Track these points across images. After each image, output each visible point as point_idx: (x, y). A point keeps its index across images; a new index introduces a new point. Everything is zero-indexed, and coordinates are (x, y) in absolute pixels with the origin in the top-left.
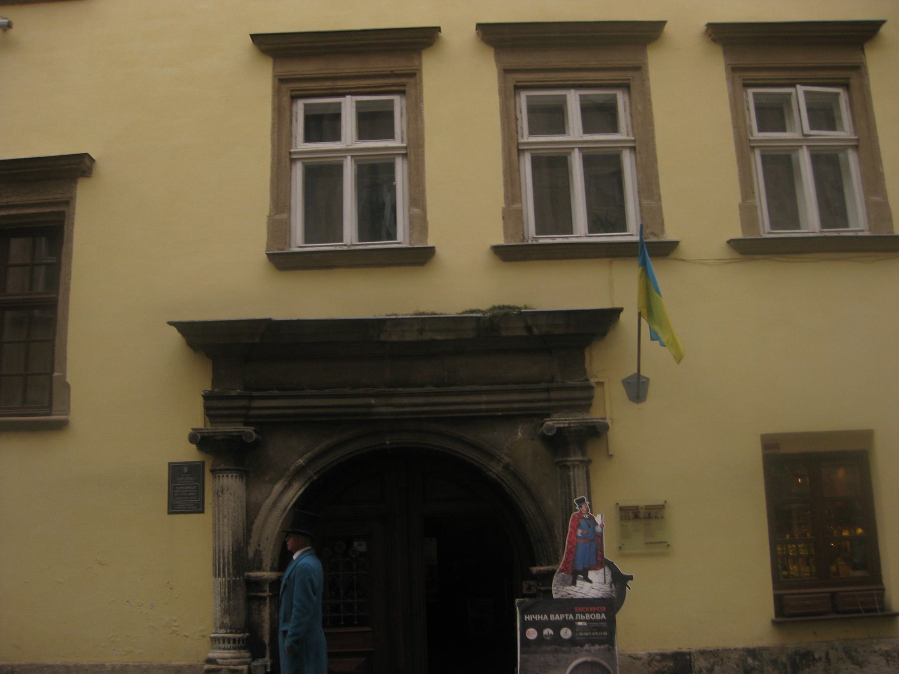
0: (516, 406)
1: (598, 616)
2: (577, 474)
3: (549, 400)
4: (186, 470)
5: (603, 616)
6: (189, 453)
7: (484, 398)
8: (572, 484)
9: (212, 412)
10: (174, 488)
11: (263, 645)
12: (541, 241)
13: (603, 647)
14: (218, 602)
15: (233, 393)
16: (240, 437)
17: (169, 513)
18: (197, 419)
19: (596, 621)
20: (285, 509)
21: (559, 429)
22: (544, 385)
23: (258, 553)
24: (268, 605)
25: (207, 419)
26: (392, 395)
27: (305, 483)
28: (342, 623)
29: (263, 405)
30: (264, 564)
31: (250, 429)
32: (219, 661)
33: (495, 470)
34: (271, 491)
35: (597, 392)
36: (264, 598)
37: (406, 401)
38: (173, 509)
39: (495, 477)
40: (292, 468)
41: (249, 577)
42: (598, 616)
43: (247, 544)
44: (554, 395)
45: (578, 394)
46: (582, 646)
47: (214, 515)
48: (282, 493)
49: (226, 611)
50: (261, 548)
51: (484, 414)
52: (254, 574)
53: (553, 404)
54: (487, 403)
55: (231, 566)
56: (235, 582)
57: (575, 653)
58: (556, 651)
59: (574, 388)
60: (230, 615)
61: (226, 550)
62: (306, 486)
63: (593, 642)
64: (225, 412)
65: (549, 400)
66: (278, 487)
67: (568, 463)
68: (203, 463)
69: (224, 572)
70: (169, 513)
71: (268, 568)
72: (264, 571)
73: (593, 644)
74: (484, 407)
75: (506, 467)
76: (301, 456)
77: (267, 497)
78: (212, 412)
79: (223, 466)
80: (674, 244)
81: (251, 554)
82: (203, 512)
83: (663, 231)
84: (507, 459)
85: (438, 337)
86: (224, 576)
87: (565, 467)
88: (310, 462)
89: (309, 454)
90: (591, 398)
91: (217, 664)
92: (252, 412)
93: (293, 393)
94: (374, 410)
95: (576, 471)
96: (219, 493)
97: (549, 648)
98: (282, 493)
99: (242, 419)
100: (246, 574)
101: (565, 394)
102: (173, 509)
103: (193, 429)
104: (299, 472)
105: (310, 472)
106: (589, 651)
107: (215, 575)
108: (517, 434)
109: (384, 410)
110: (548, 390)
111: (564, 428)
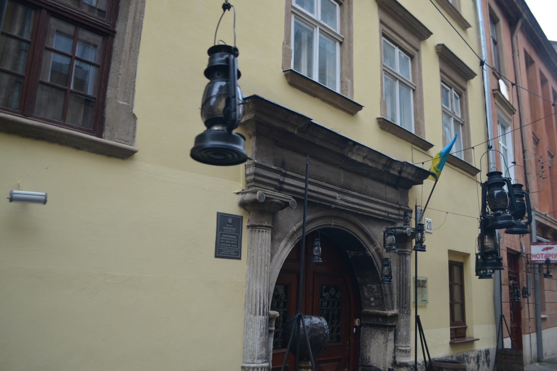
6: (232, 208)
7: (378, 207)
9: (258, 178)
17: (216, 257)
28: (280, 346)
39: (371, 255)
54: (379, 210)
67: (407, 253)
68: (242, 217)
70: (216, 257)
78: (258, 178)
82: (240, 259)
85: (370, 164)
86: (263, 315)
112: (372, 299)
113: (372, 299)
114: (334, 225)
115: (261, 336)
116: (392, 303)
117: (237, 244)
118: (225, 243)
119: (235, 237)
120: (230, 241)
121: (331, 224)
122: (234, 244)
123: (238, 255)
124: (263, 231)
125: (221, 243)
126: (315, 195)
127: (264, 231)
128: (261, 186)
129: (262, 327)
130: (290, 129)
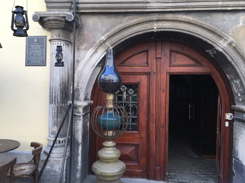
4: (36, 41)
9: (50, 5)
11: (78, 143)
14: (51, 119)
16: (65, 17)
17: (26, 66)
24: (81, 121)
30: (80, 97)
33: (221, 45)
36: (80, 116)
39: (221, 50)
40: (98, 41)
50: (79, 87)
64: (57, 5)
69: (55, 101)
70: (26, 66)
71: (83, 99)
75: (230, 44)
84: (231, 39)
86: (55, 104)
88: (109, 37)
89: (108, 34)
105: (108, 44)
108: (239, 23)
109: (155, 5)
112: (239, 95)
113: (239, 95)
114: (157, 29)
115: (53, 118)
117: (42, 56)
118: (33, 56)
121: (153, 29)
122: (39, 56)
124: (53, 44)
125: (29, 56)
126: (118, 5)
127: (54, 43)
129: (54, 112)
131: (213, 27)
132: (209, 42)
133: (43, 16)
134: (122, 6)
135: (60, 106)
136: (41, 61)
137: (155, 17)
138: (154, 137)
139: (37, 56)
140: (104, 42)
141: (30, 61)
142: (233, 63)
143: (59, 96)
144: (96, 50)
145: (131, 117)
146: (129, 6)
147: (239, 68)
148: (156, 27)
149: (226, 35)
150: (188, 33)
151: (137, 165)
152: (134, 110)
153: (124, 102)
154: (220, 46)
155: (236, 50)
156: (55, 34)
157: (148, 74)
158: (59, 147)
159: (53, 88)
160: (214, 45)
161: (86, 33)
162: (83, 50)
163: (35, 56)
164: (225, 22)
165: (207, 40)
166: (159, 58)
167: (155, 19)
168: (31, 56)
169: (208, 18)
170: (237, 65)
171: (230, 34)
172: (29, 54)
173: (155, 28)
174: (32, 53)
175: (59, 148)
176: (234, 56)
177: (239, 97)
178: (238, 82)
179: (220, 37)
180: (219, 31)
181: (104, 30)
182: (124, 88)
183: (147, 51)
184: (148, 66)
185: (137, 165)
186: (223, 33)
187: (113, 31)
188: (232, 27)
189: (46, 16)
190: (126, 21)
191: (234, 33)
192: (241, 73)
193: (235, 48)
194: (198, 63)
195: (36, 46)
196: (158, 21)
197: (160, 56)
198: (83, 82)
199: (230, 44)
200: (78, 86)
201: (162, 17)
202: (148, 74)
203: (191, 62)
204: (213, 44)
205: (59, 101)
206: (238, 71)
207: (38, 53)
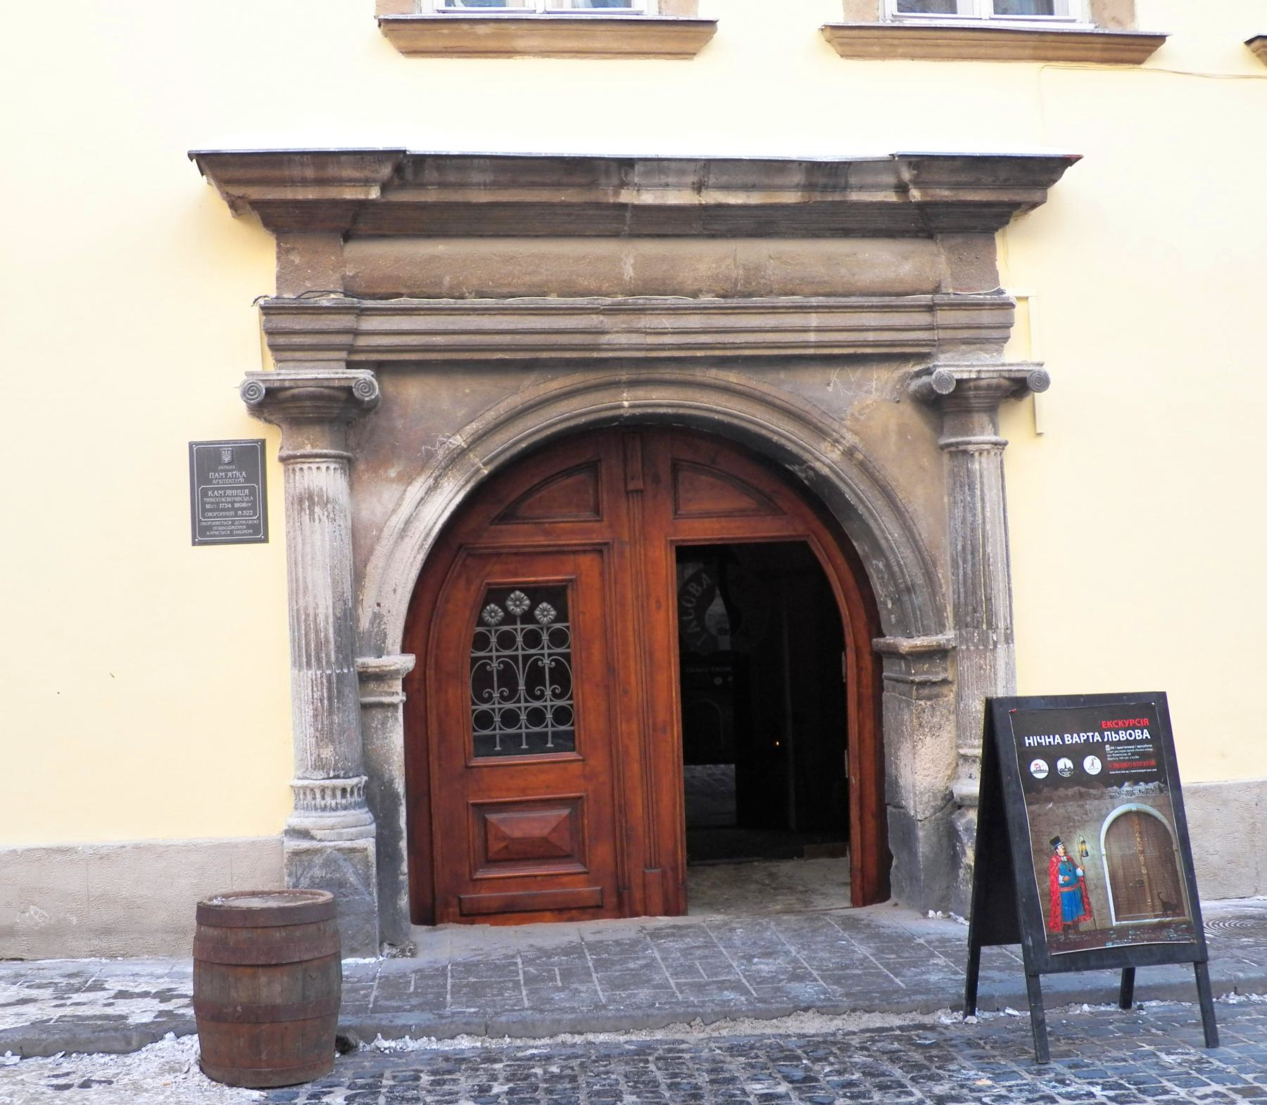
0: (871, 336)
1: (1138, 735)
2: (982, 466)
3: (930, 328)
5: (1146, 734)
6: (234, 423)
7: (814, 320)
8: (978, 486)
9: (281, 340)
10: (204, 493)
11: (395, 796)
12: (908, 23)
13: (1151, 786)
15: (324, 302)
18: (251, 358)
19: (1136, 742)
20: (428, 535)
21: (959, 381)
22: (926, 299)
23: (377, 617)
25: (268, 353)
26: (641, 311)
27: (467, 482)
29: (385, 329)
30: (389, 641)
31: (365, 374)
32: (318, 834)
33: (826, 458)
34: (402, 498)
35: (1019, 311)
36: (393, 706)
37: (667, 322)
38: (203, 534)
39: (825, 471)
40: (441, 453)
41: (364, 666)
42: (1138, 735)
43: (357, 601)
44: (943, 317)
45: (986, 317)
46: (1121, 786)
47: (291, 547)
48: (422, 501)
49: (326, 735)
51: (811, 351)
52: (372, 662)
53: (941, 334)
54: (819, 330)
55: (332, 646)
56: (340, 677)
57: (1112, 797)
58: (1081, 795)
59: (978, 306)
60: (332, 741)
61: (321, 618)
62: (468, 488)
63: (1136, 779)
65: (930, 328)
66: (416, 489)
67: (970, 448)
68: (263, 442)
71: (398, 647)
72: (388, 654)
73: (1136, 783)
74: (812, 337)
75: (849, 453)
76: (458, 430)
77: (394, 511)
78: (281, 340)
79: (308, 449)
80: (1158, 40)
81: (365, 623)
82: (265, 540)
83: (1132, 15)
84: (850, 439)
87: (960, 453)
88: (479, 439)
89: (474, 425)
90: (1007, 326)
91: (313, 838)
92: (362, 342)
93: (444, 302)
94: (604, 339)
95: (984, 459)
96: (306, 502)
97: (1070, 792)
98: (422, 501)
99: (344, 355)
100: (360, 661)
101: (961, 317)
102: (203, 534)
103: (248, 374)
104: (457, 457)
106: (1132, 793)
107: (297, 663)
109: (623, 339)
110: (931, 308)
111: (969, 380)
114: (631, 407)
115: (315, 716)
116: (939, 611)
117: (253, 508)
119: (247, 491)
120: (233, 503)
121: (621, 407)
122: (242, 509)
123: (257, 532)
124: (301, 469)
125: (204, 510)
126: (507, 339)
127: (305, 466)
128: (298, 355)
130: (350, 194)
131: (798, 404)
132: (790, 446)
133: (277, 384)
134: (522, 342)
135: (338, 675)
136: (249, 527)
137: (624, 376)
138: (636, 767)
139: (236, 510)
140: (463, 452)
141: (210, 528)
142: (861, 510)
143: (332, 640)
144: (436, 479)
145: (549, 703)
146: (543, 342)
147: (879, 525)
148: (627, 401)
149: (836, 426)
150: (726, 419)
151: (581, 869)
152: (561, 676)
153: (520, 652)
154: (823, 458)
155: (867, 470)
156: (308, 439)
157: (599, 550)
158: (345, 808)
159: (307, 615)
160: (806, 456)
161: (399, 424)
162: (392, 481)
163: (228, 510)
164: (830, 389)
165: (783, 441)
166: (637, 491)
167: (624, 378)
168: (210, 510)
169: (782, 375)
170: (872, 514)
171: (848, 423)
172: (204, 504)
173: (626, 404)
174: (212, 500)
175: (343, 813)
176: (862, 487)
177: (890, 612)
178: (881, 565)
179: (820, 432)
180: (815, 416)
181: (461, 413)
182: (521, 600)
183: (593, 467)
184: (601, 521)
185: (581, 869)
186: (828, 422)
187: (491, 416)
188: (851, 403)
189: (287, 384)
190: (531, 388)
191: (857, 420)
192: (887, 540)
193: (863, 466)
194: (768, 506)
195: (230, 474)
196: (633, 384)
197: (640, 485)
198: (395, 591)
199: (849, 453)
200: (379, 605)
201: (644, 374)
202: (599, 550)
203: (746, 502)
204: (801, 453)
205: (333, 658)
206: (877, 532)
207: (237, 499)
